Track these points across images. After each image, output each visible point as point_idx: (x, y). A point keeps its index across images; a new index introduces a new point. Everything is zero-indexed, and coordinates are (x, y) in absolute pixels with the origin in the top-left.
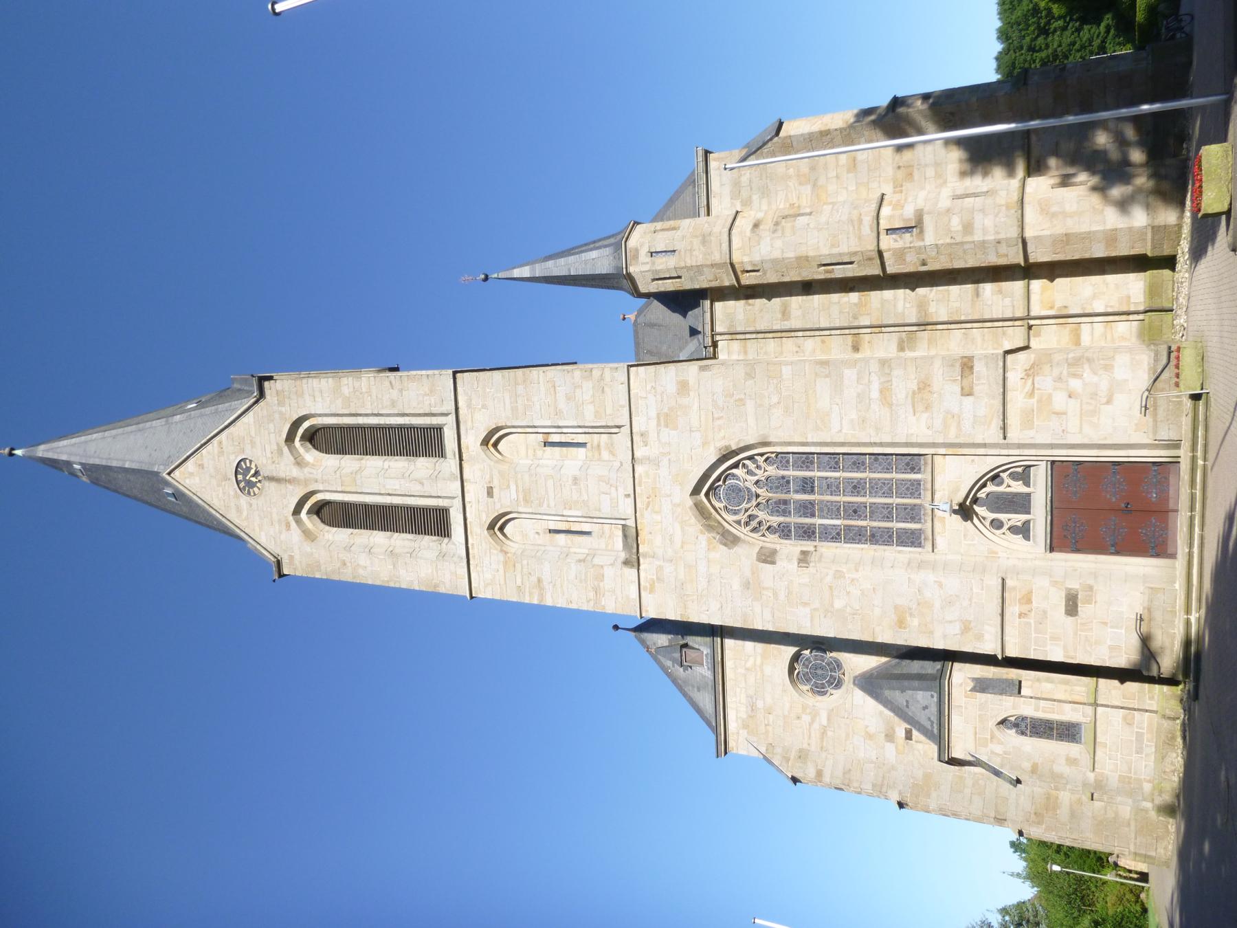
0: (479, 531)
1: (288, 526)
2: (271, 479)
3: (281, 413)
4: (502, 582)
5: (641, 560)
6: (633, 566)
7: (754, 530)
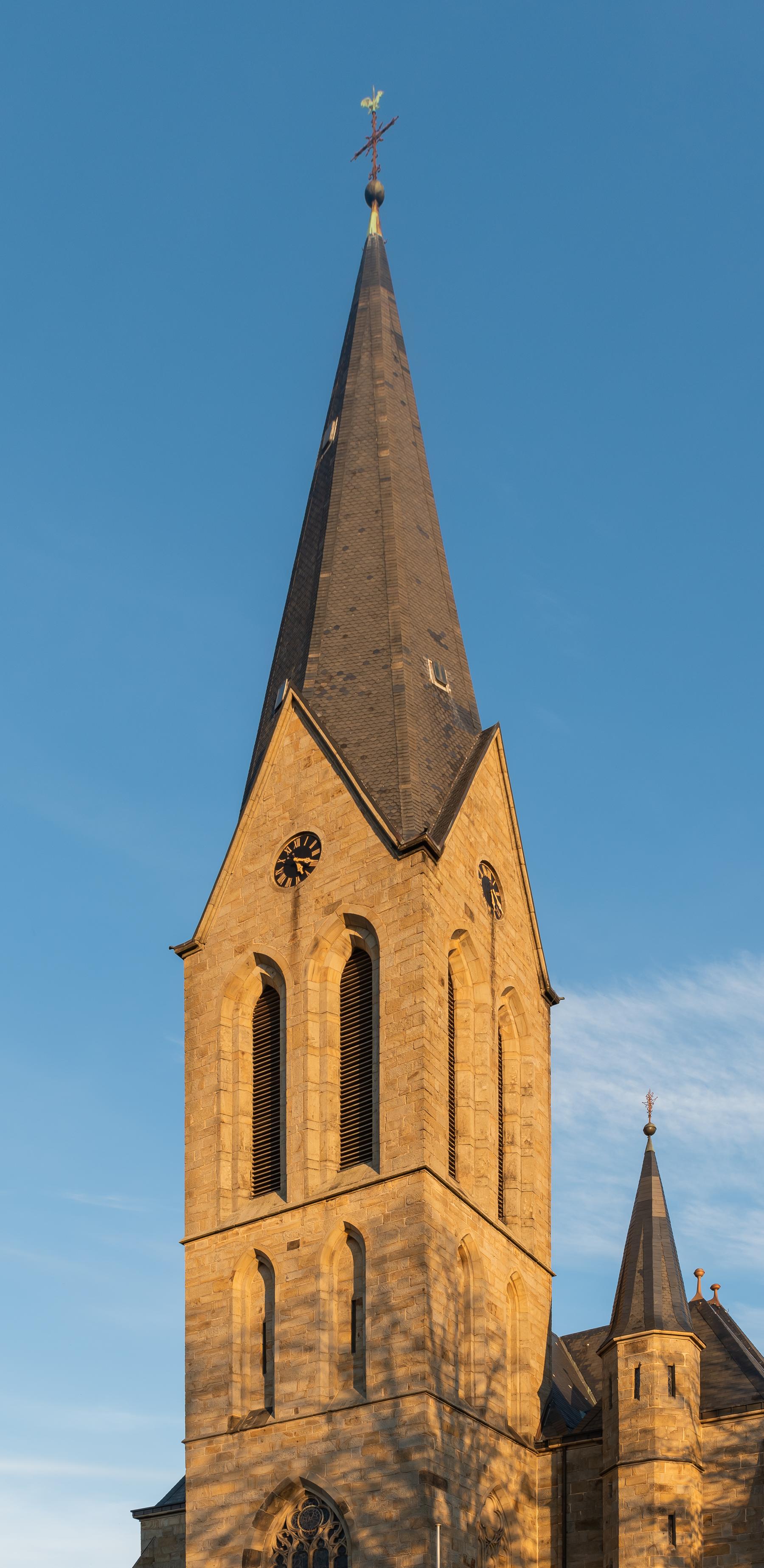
0: (252, 1239)
1: (240, 950)
2: (296, 903)
3: (380, 894)
4: (202, 1280)
5: (236, 1435)
6: (230, 1426)
7: (279, 1543)
